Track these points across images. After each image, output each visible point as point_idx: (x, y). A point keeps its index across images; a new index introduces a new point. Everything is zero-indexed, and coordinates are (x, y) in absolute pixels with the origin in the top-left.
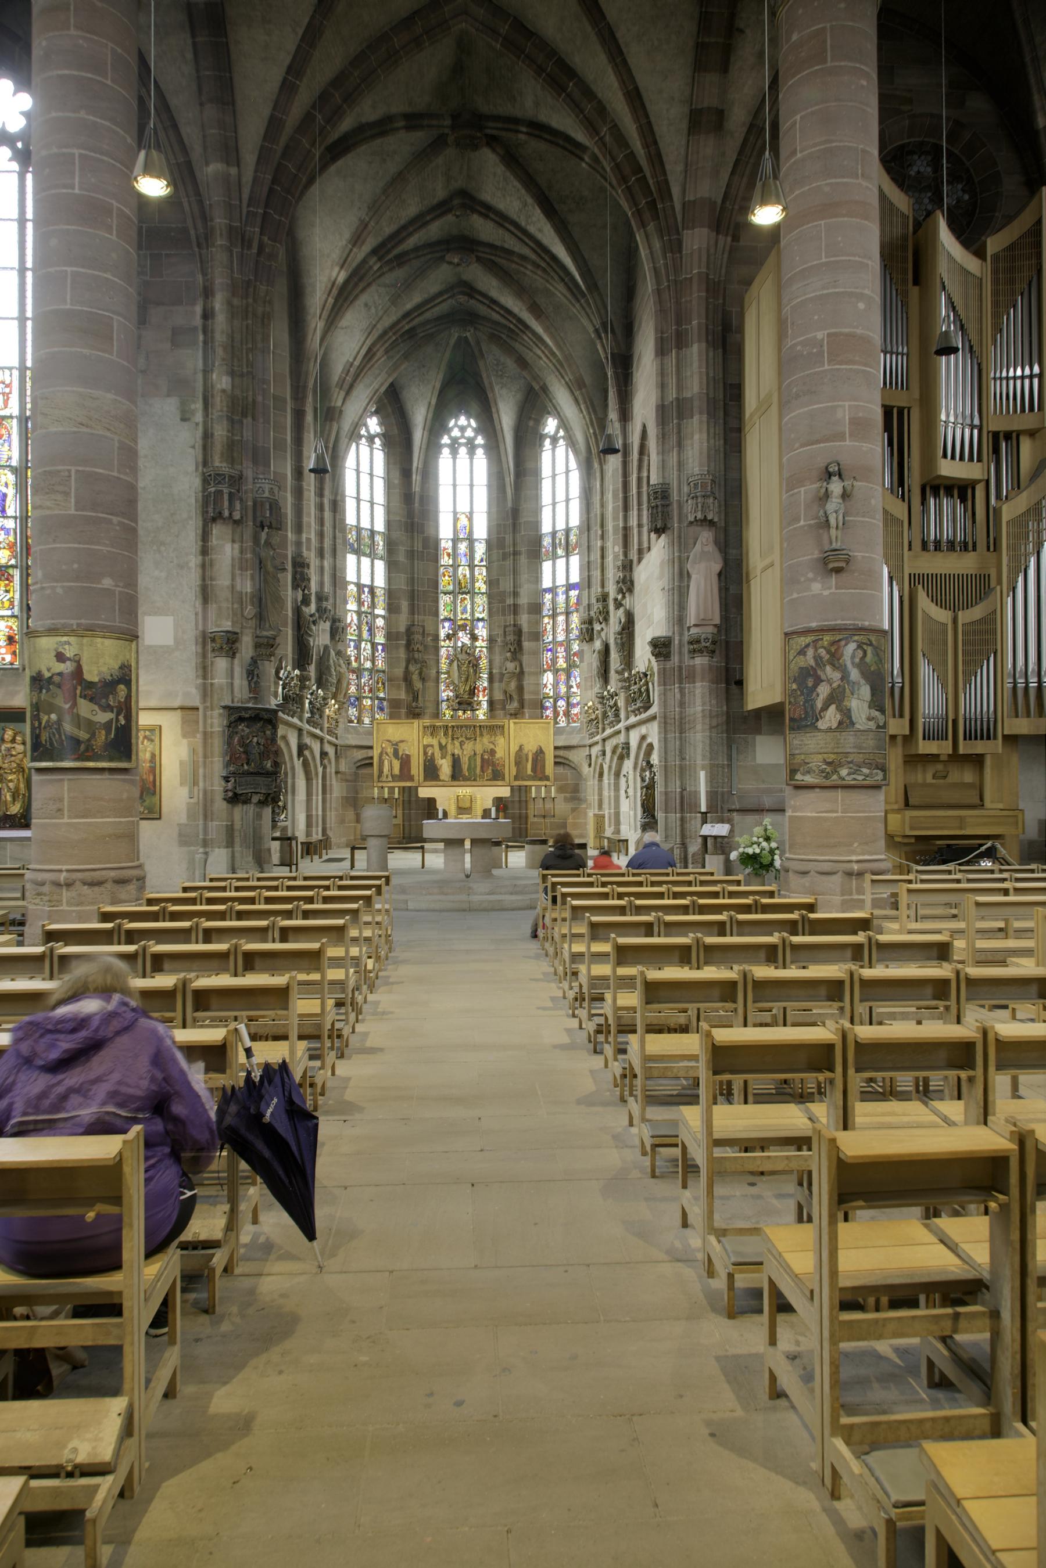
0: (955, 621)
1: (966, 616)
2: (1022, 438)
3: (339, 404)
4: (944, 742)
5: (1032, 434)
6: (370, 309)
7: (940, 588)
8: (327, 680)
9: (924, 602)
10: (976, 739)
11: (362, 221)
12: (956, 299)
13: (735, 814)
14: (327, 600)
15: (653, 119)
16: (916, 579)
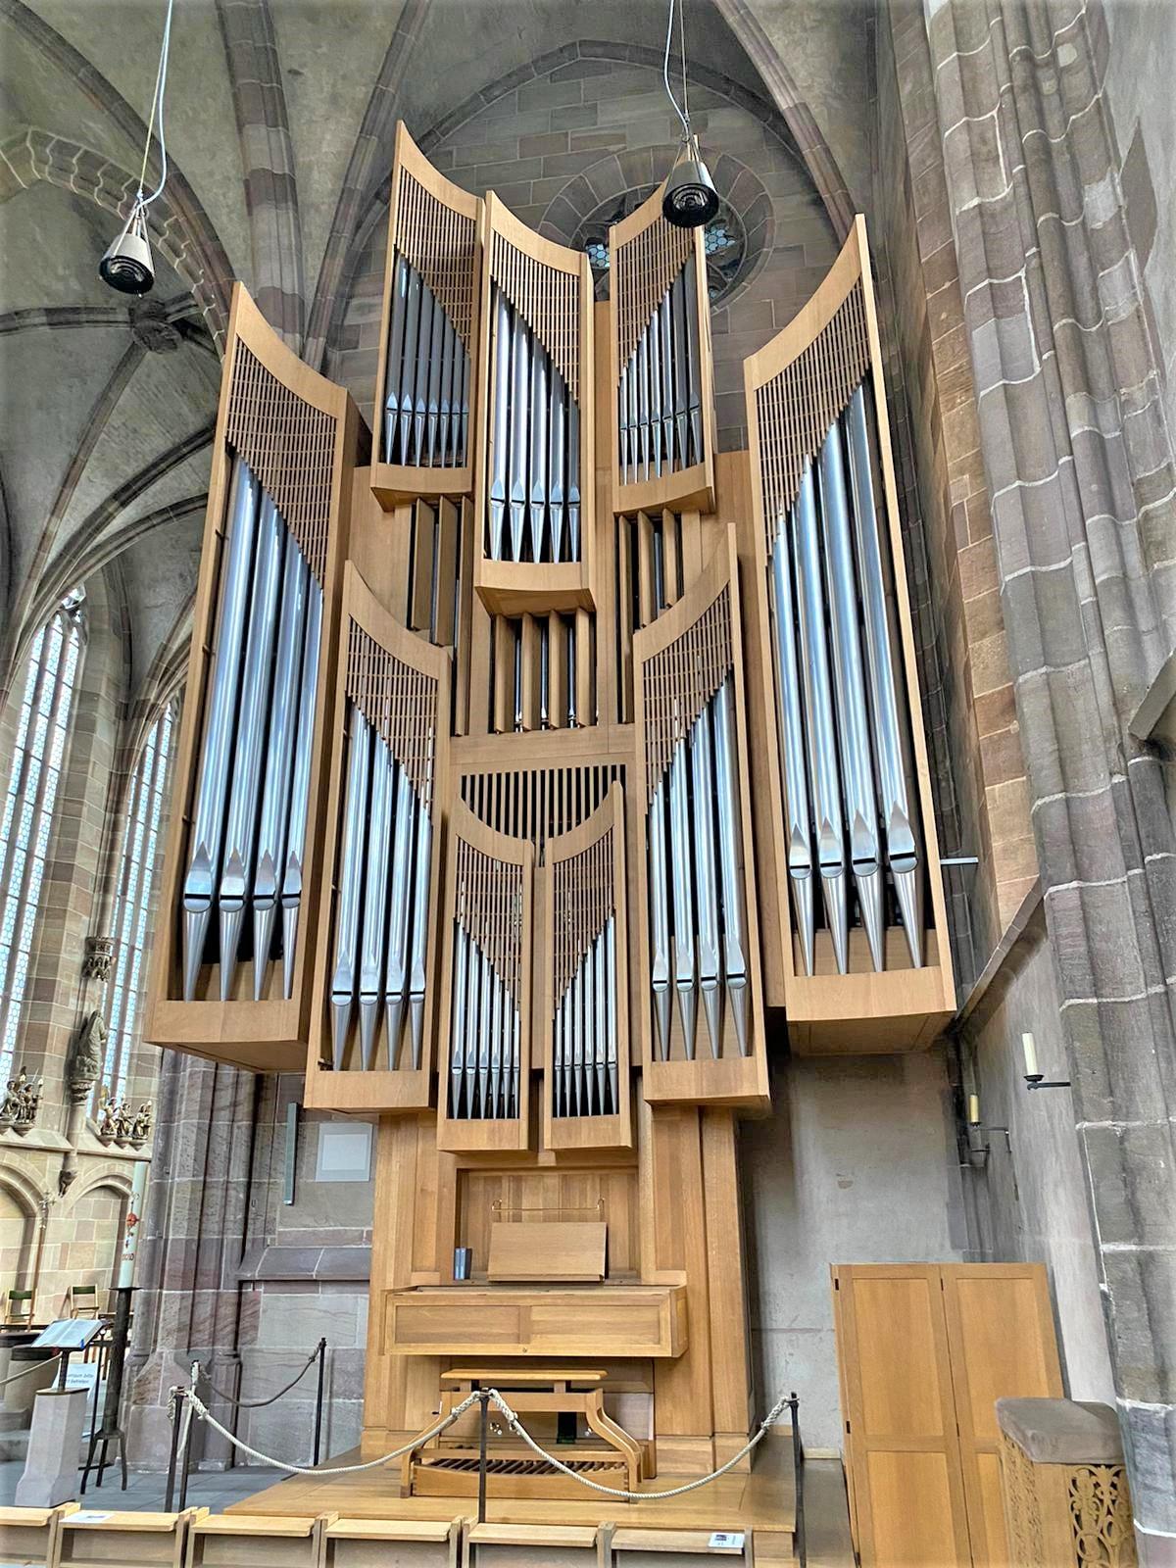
0: (539, 862)
1: (560, 848)
2: (684, 519)
3: (152, 697)
4: (507, 1122)
5: (709, 509)
6: (185, 579)
7: (500, 800)
8: (83, 1063)
9: (468, 827)
10: (584, 1113)
11: (71, 456)
12: (527, 311)
13: (261, 1289)
14: (102, 948)
15: (208, 211)
16: (479, 792)
